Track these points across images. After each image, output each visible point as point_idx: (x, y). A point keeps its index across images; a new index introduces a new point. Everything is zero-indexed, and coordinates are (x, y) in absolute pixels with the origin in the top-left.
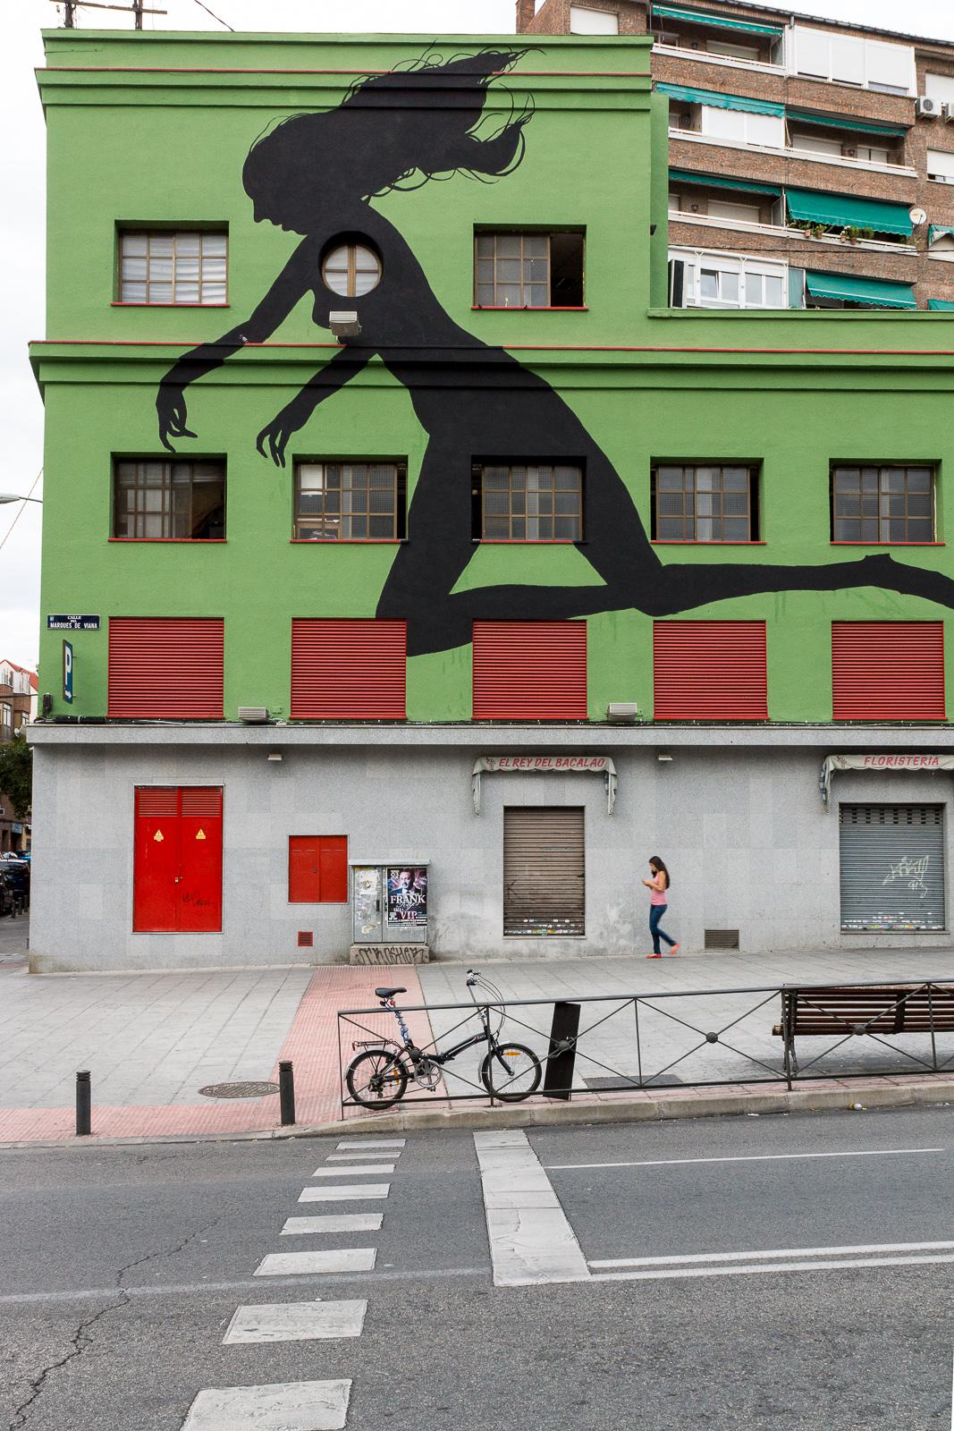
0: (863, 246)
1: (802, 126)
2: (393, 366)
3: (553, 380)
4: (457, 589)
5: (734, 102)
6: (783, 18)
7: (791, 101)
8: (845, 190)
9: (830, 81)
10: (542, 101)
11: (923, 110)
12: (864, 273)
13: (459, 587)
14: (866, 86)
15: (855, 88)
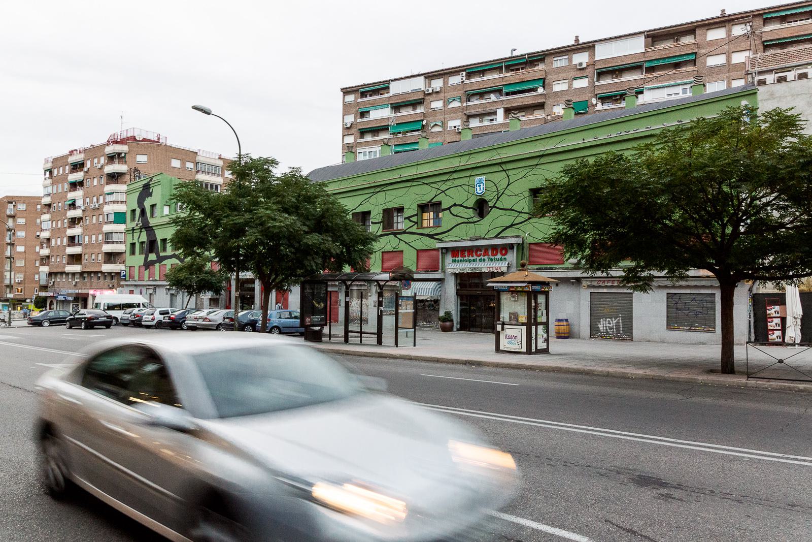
0: (408, 135)
1: (396, 107)
2: (145, 228)
3: (154, 228)
4: (148, 260)
5: (377, 107)
6: (388, 82)
7: (390, 102)
8: (403, 121)
9: (401, 94)
10: (154, 185)
11: (426, 92)
12: (408, 142)
13: (148, 260)
14: (410, 92)
15: (408, 93)
